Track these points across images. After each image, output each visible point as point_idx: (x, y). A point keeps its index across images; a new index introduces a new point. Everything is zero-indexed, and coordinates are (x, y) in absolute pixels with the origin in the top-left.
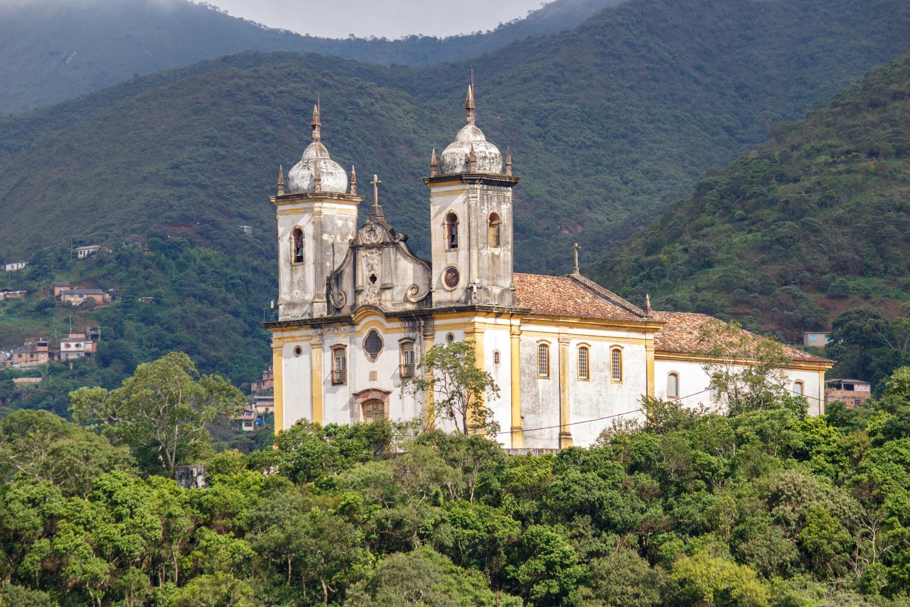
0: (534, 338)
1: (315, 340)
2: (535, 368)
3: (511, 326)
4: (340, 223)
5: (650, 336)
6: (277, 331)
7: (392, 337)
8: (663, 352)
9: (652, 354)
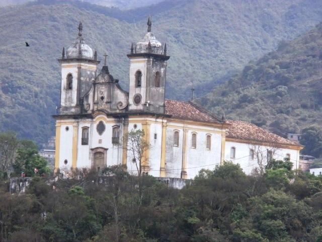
0: (172, 129)
1: (75, 124)
2: (172, 142)
3: (163, 122)
4: (89, 73)
5: (224, 131)
6: (58, 119)
8: (230, 137)
9: (224, 139)
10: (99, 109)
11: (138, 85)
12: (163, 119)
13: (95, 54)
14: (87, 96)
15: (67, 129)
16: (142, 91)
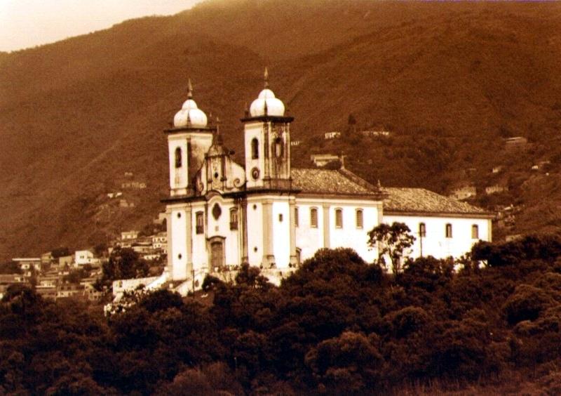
1: (188, 209)
3: (289, 200)
5: (380, 203)
7: (226, 207)
9: (381, 213)
10: (213, 188)
11: (256, 156)
12: (289, 195)
13: (209, 122)
14: (199, 173)
15: (179, 215)
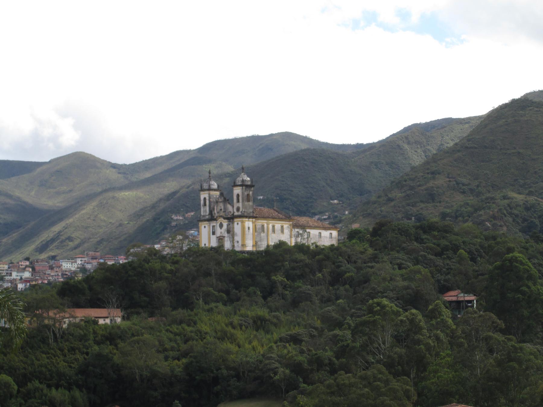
2: (260, 231)
7: (225, 224)
11: (238, 201)
13: (218, 186)
15: (205, 227)
16: (240, 205)
